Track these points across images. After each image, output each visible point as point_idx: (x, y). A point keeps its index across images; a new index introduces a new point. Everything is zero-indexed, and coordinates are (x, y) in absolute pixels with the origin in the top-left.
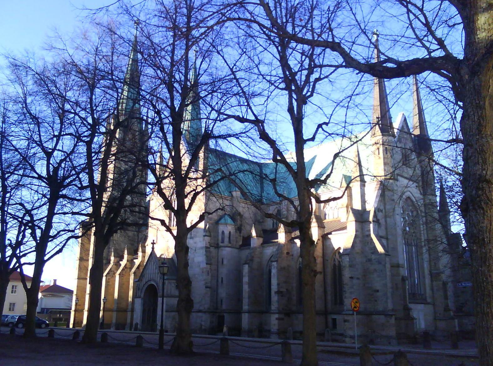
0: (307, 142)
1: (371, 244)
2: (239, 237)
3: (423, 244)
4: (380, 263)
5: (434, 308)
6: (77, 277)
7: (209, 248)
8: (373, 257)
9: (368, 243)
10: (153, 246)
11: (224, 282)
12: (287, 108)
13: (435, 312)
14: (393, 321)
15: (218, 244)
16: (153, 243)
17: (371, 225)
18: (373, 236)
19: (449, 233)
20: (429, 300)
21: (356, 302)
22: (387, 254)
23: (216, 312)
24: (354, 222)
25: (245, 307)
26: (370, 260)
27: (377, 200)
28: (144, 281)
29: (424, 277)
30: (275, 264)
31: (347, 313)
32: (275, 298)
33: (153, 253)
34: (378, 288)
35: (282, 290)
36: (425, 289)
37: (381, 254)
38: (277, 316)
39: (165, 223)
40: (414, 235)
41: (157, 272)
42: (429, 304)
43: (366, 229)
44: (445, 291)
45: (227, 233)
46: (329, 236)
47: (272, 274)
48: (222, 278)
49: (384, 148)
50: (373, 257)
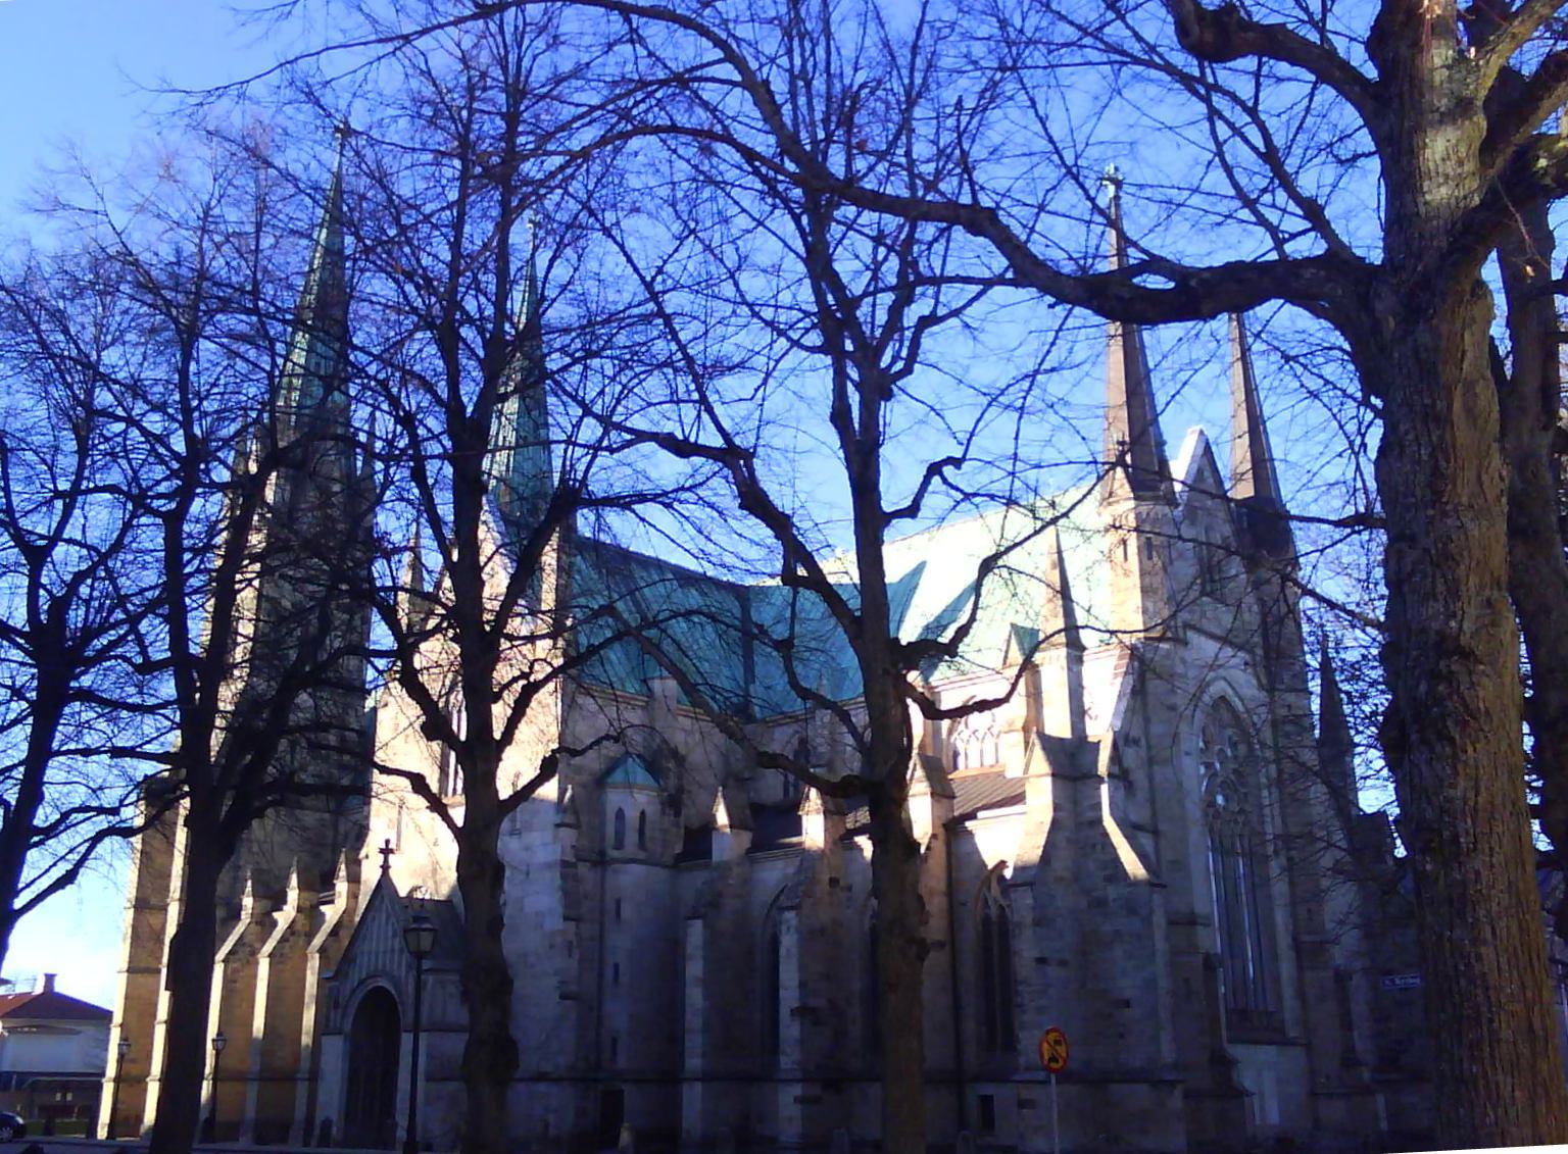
0: (894, 521)
2: (674, 830)
3: (1270, 849)
4: (1132, 912)
6: (125, 966)
7: (574, 865)
8: (1112, 892)
9: (1094, 846)
10: (386, 860)
11: (624, 979)
12: (829, 411)
14: (1176, 1101)
15: (602, 853)
16: (386, 851)
17: (1104, 789)
18: (1110, 824)
19: (1354, 812)
20: (1292, 1033)
21: (1057, 1042)
22: (1155, 883)
23: (595, 1080)
24: (1049, 780)
25: (694, 1063)
26: (1101, 903)
27: (1123, 707)
28: (355, 977)
29: (1275, 957)
30: (790, 915)
31: (1027, 1076)
32: (790, 1030)
33: (385, 883)
34: (1128, 994)
35: (812, 1002)
36: (1280, 998)
37: (1136, 883)
38: (797, 1090)
39: (427, 786)
40: (1241, 819)
41: (397, 947)
42: (1291, 1043)
43: (1086, 804)
44: (1344, 1000)
45: (632, 816)
46: (969, 824)
47: (783, 951)
48: (616, 966)
50: (1112, 892)
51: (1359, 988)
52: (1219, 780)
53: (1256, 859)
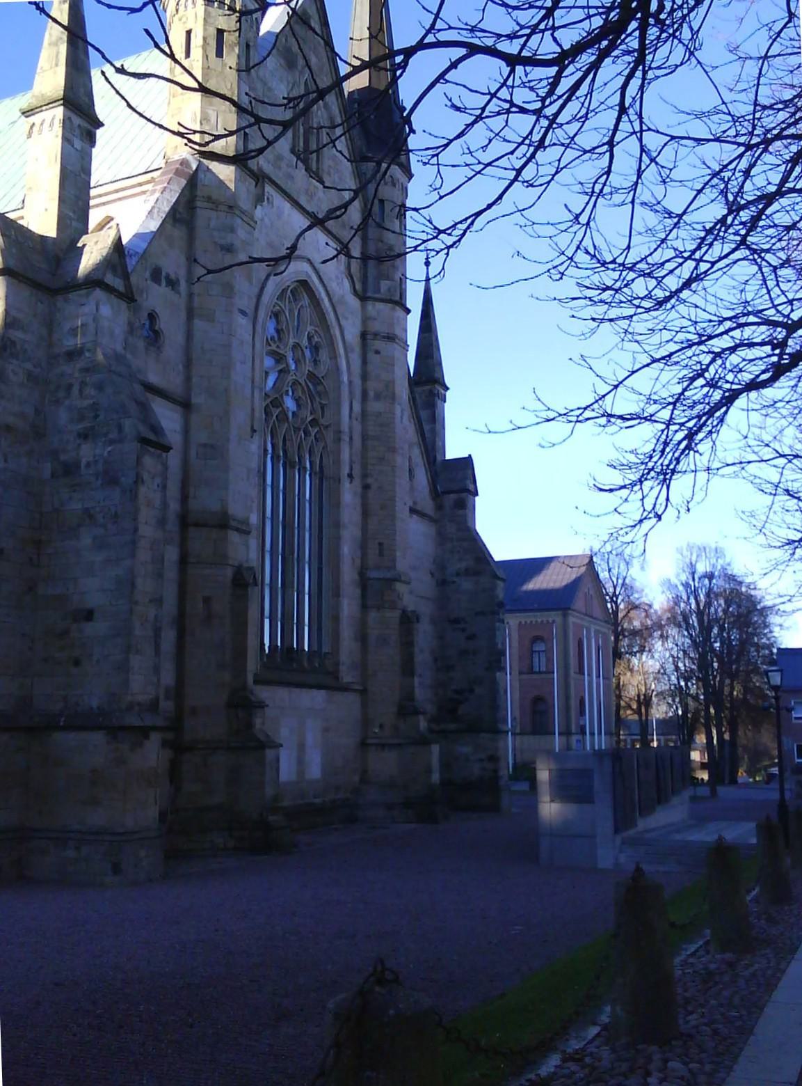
1: (81, 391)
3: (345, 470)
4: (110, 479)
5: (364, 706)
9: (70, 387)
13: (366, 722)
14: (153, 754)
19: (439, 458)
20: (347, 677)
26: (70, 470)
29: (337, 593)
34: (94, 599)
40: (313, 431)
42: (345, 689)
43: (67, 326)
44: (407, 644)
49: (213, 32)
51: (424, 634)
52: (291, 378)
53: (325, 480)
